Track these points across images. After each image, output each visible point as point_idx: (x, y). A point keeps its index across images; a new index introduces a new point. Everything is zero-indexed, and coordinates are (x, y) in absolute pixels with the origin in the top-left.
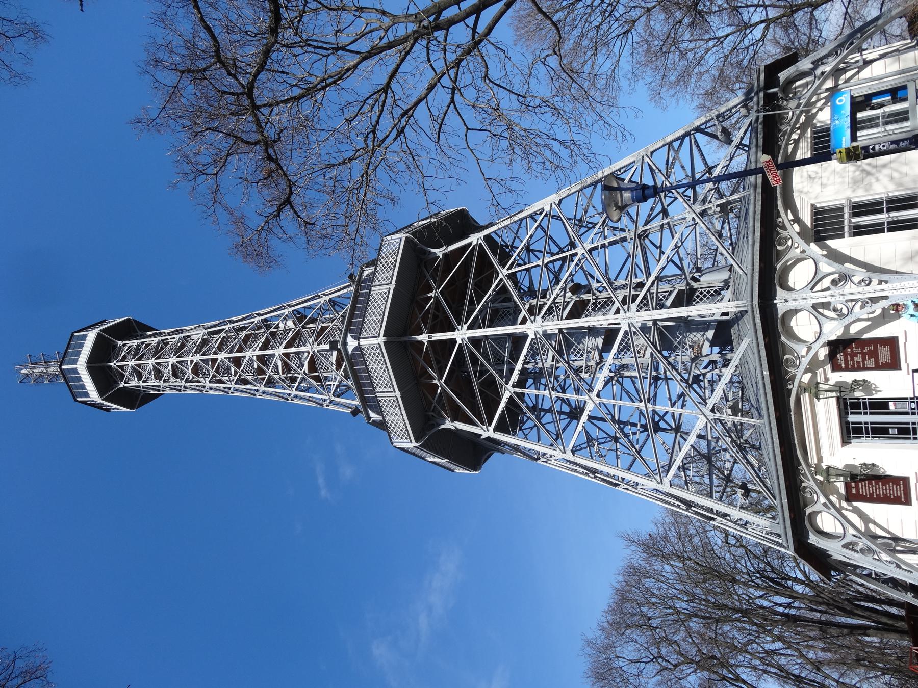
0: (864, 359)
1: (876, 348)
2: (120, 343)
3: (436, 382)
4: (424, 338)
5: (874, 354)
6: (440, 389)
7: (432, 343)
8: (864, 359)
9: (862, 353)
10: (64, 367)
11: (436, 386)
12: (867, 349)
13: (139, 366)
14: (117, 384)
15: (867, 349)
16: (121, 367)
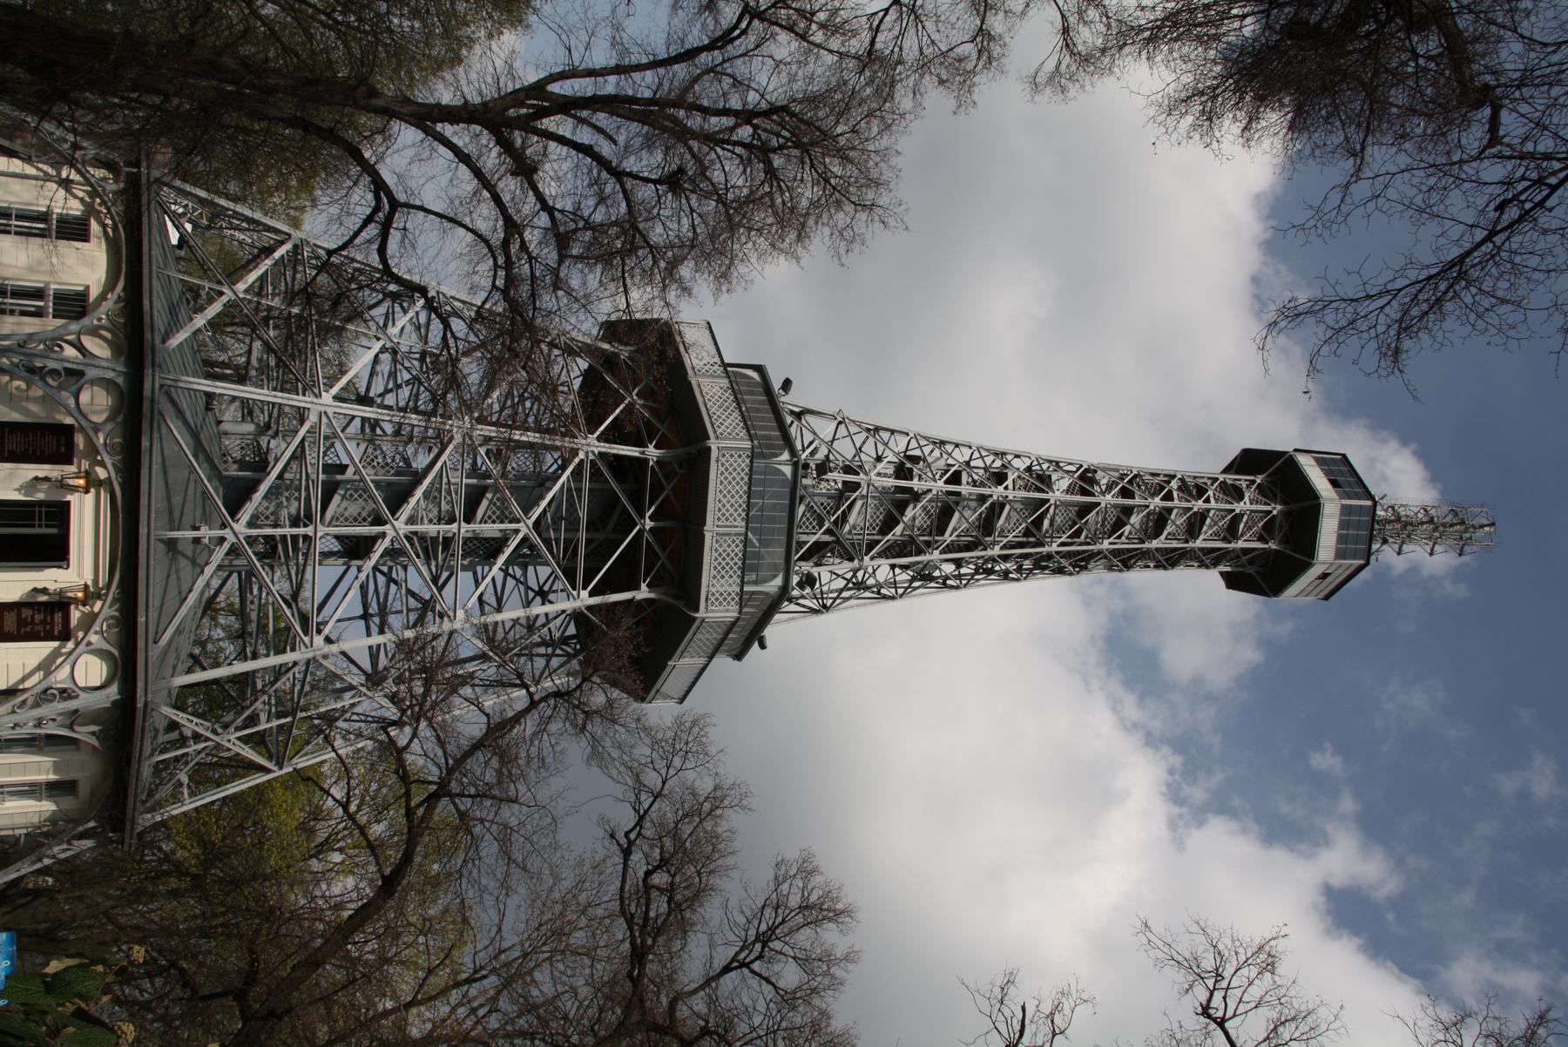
0: (33, 617)
1: (19, 631)
2: (1251, 570)
3: (649, 524)
4: (643, 593)
5: (22, 622)
6: (648, 515)
7: (638, 588)
8: (33, 617)
9: (33, 623)
10: (1362, 562)
12: (28, 629)
13: (1224, 540)
14: (1286, 514)
15: (28, 629)
16: (1261, 539)
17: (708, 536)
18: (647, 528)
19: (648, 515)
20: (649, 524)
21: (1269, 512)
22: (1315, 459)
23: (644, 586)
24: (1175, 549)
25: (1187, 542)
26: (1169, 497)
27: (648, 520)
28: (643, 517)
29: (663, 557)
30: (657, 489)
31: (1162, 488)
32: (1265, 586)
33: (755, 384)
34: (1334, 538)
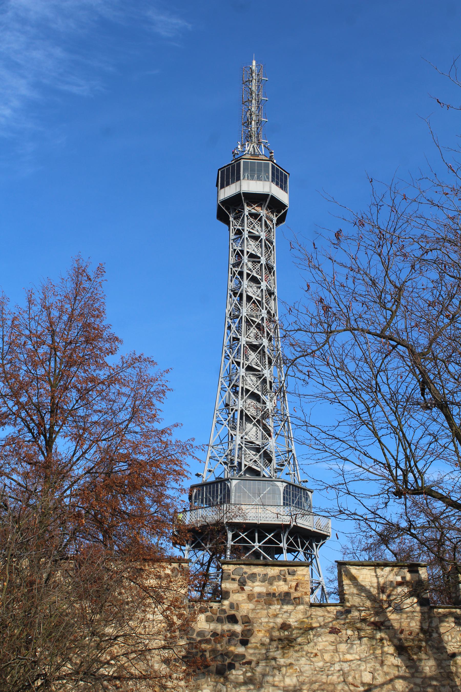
2: (275, 219)
6: (253, 544)
11: (254, 542)
13: (261, 241)
16: (260, 220)
17: (260, 522)
18: (258, 544)
19: (253, 544)
20: (257, 545)
21: (247, 216)
22: (221, 188)
23: (281, 545)
24: (265, 268)
25: (262, 264)
26: (241, 274)
27: (255, 544)
28: (254, 547)
29: (270, 536)
30: (243, 540)
31: (238, 253)
32: (283, 212)
33: (199, 491)
34: (258, 182)
